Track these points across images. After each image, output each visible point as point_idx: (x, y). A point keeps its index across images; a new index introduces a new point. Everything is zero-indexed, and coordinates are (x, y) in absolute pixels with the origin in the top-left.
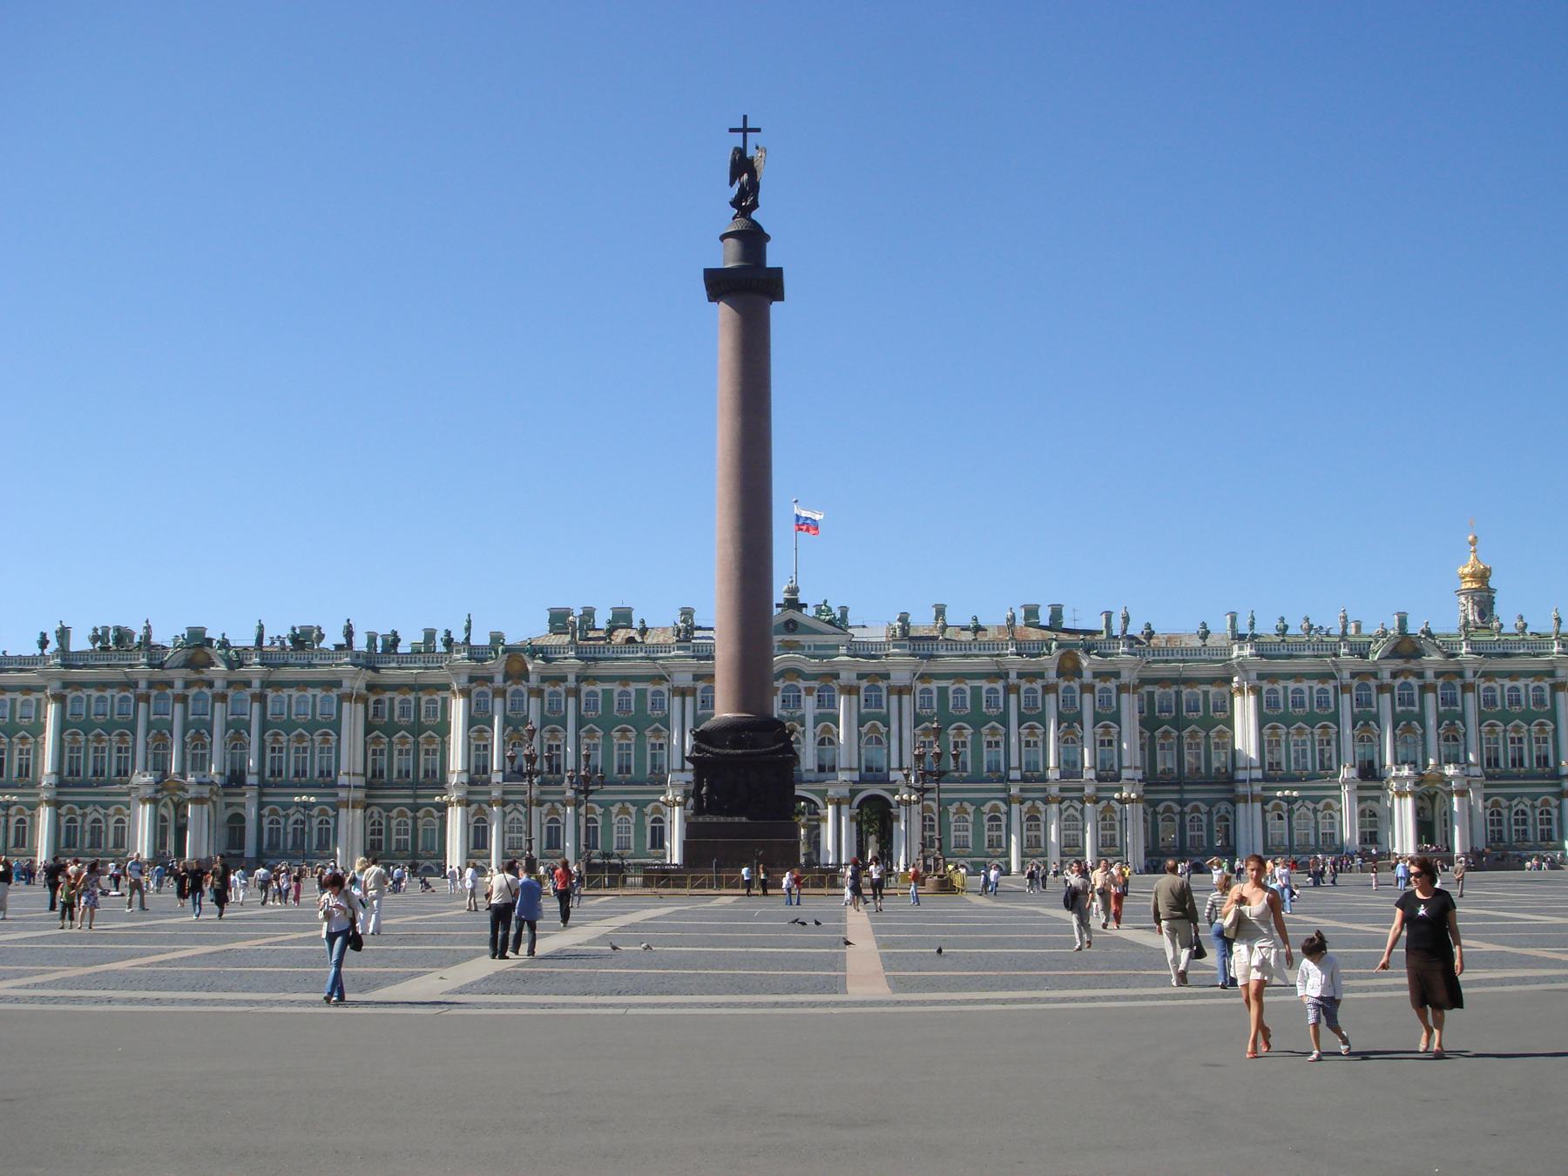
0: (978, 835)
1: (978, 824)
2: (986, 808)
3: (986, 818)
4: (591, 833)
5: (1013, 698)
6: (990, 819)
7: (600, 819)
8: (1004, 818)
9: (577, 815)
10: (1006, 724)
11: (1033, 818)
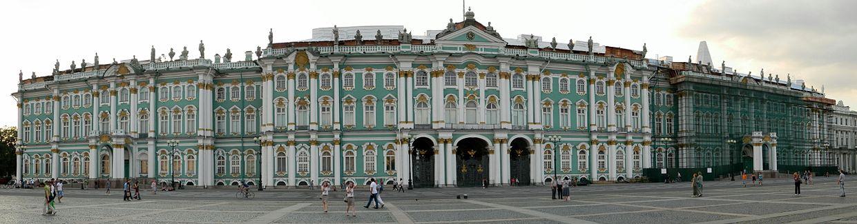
0: (575, 161)
1: (574, 156)
2: (579, 147)
3: (578, 152)
4: (350, 160)
5: (592, 86)
6: (580, 153)
7: (355, 153)
8: (588, 152)
9: (341, 150)
10: (589, 101)
11: (601, 152)
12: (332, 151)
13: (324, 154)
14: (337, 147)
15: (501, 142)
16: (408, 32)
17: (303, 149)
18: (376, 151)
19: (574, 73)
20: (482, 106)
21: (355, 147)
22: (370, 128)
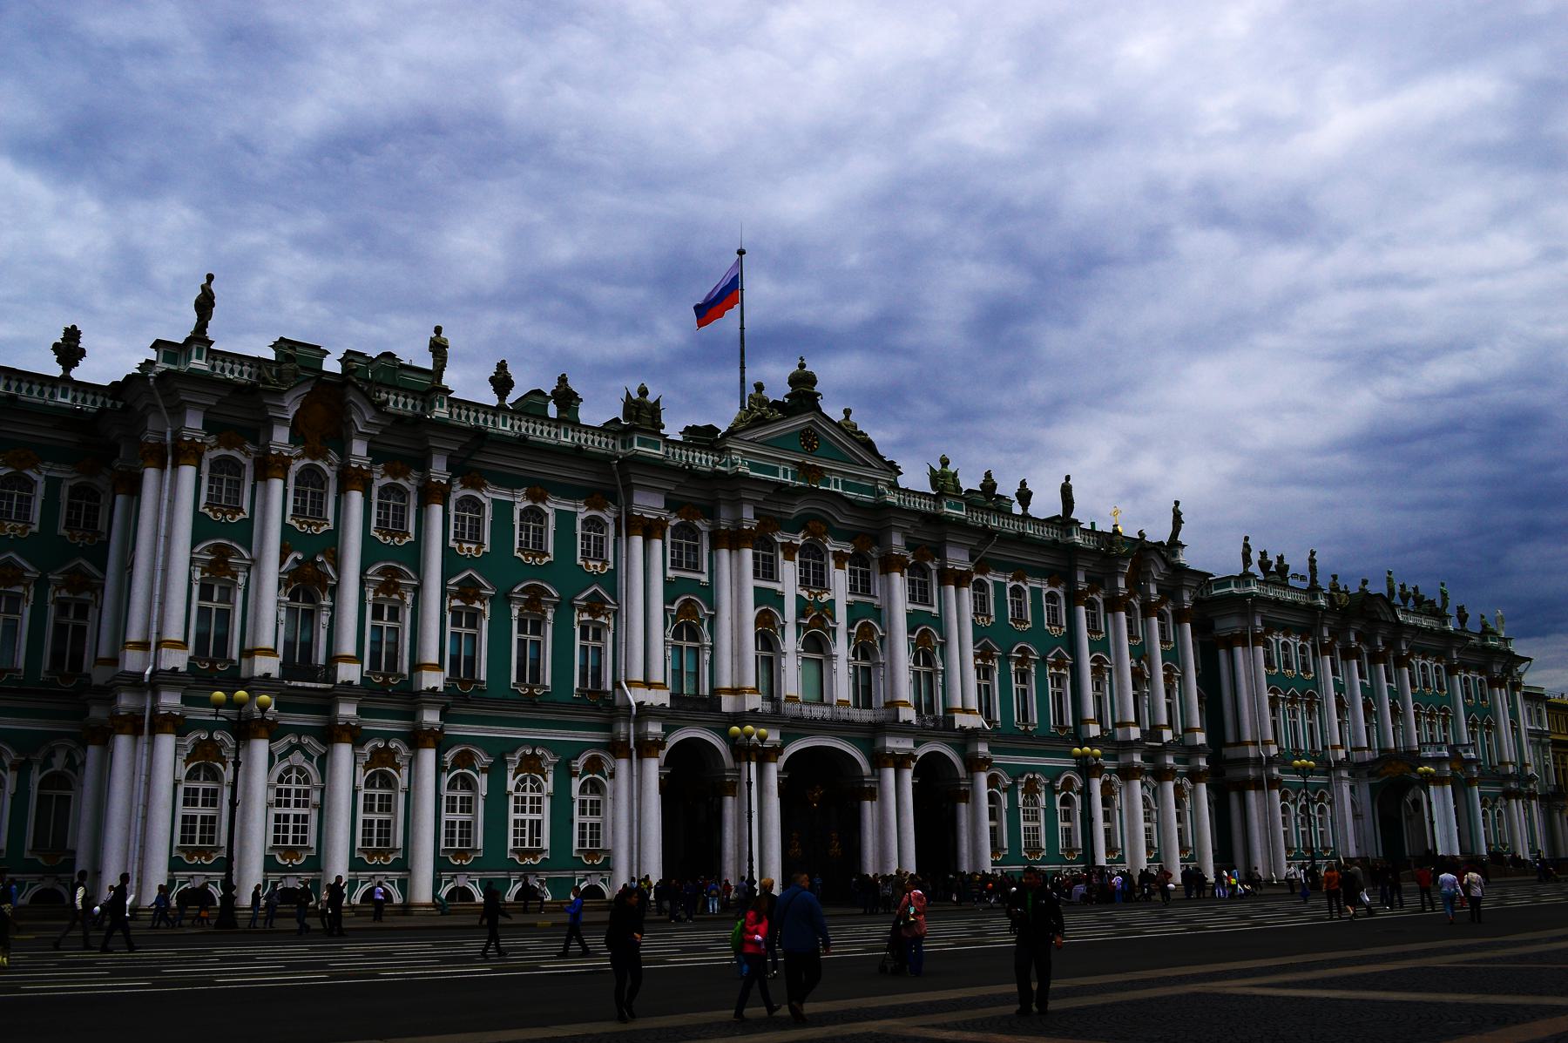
3: (1058, 798)
7: (482, 781)
8: (1078, 799)
9: (440, 768)
10: (1073, 648)
12: (405, 772)
13: (369, 783)
14: (428, 757)
15: (900, 762)
16: (651, 398)
17: (297, 758)
18: (550, 777)
19: (1037, 572)
20: (842, 648)
21: (483, 759)
22: (531, 693)
